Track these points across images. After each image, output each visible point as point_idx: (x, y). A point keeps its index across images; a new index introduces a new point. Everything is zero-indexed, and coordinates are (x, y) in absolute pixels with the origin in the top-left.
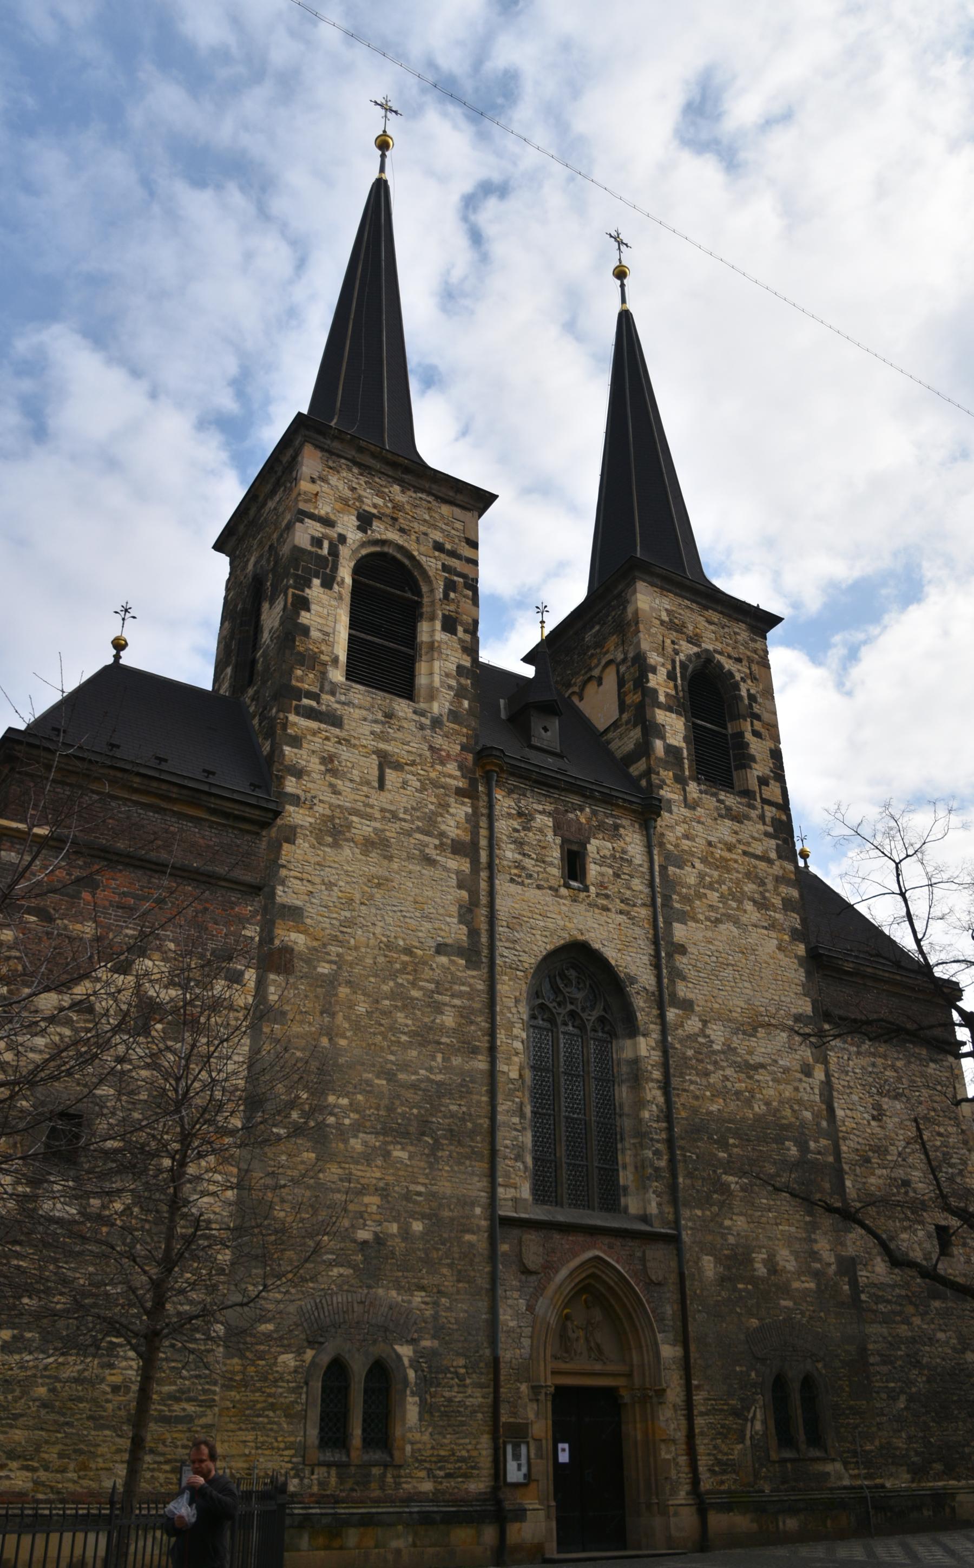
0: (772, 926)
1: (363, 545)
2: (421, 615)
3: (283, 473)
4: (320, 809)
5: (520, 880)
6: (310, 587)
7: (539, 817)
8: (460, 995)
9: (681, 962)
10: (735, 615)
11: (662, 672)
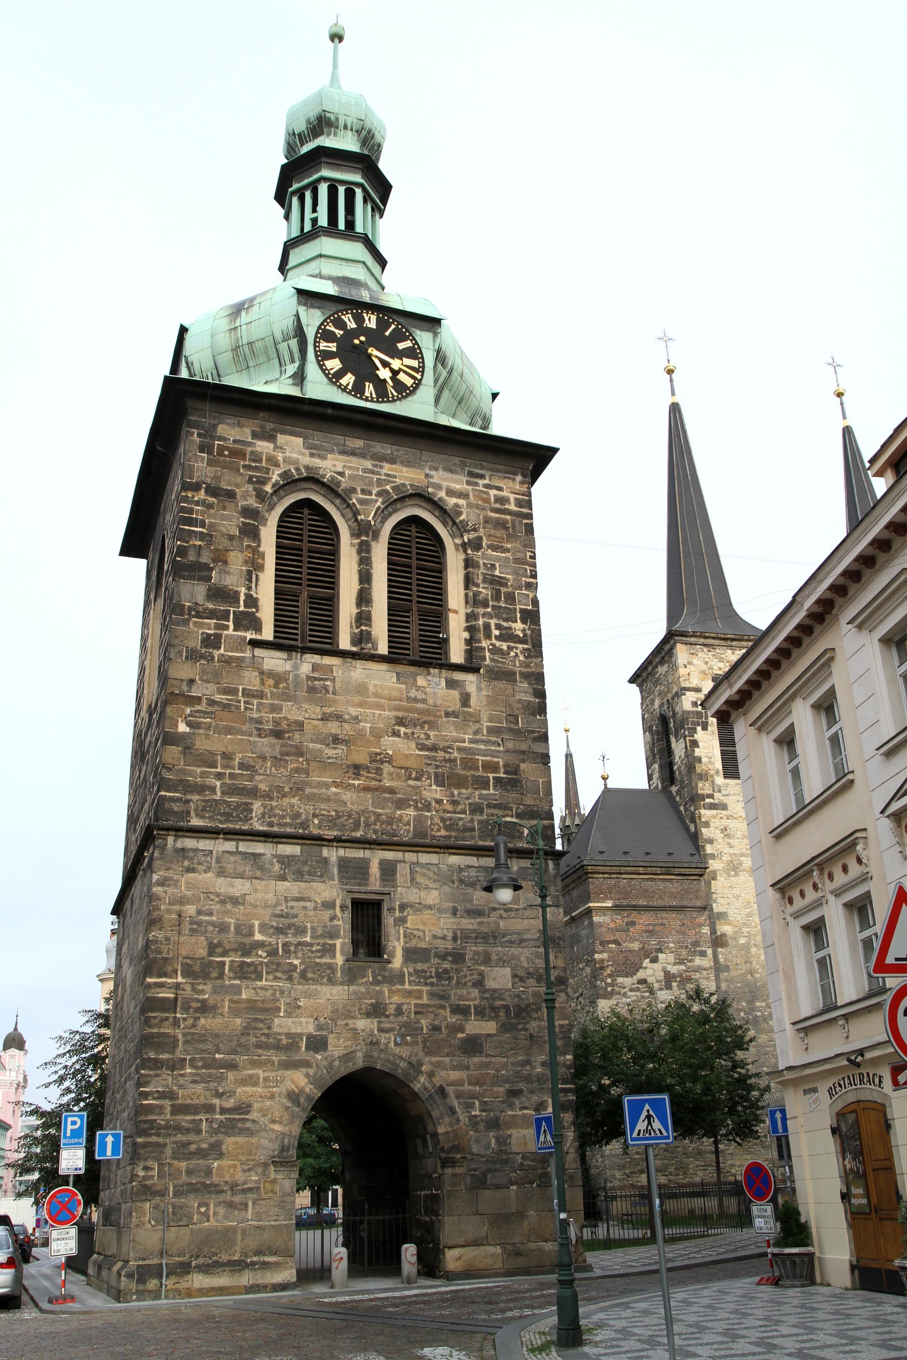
4: (725, 858)
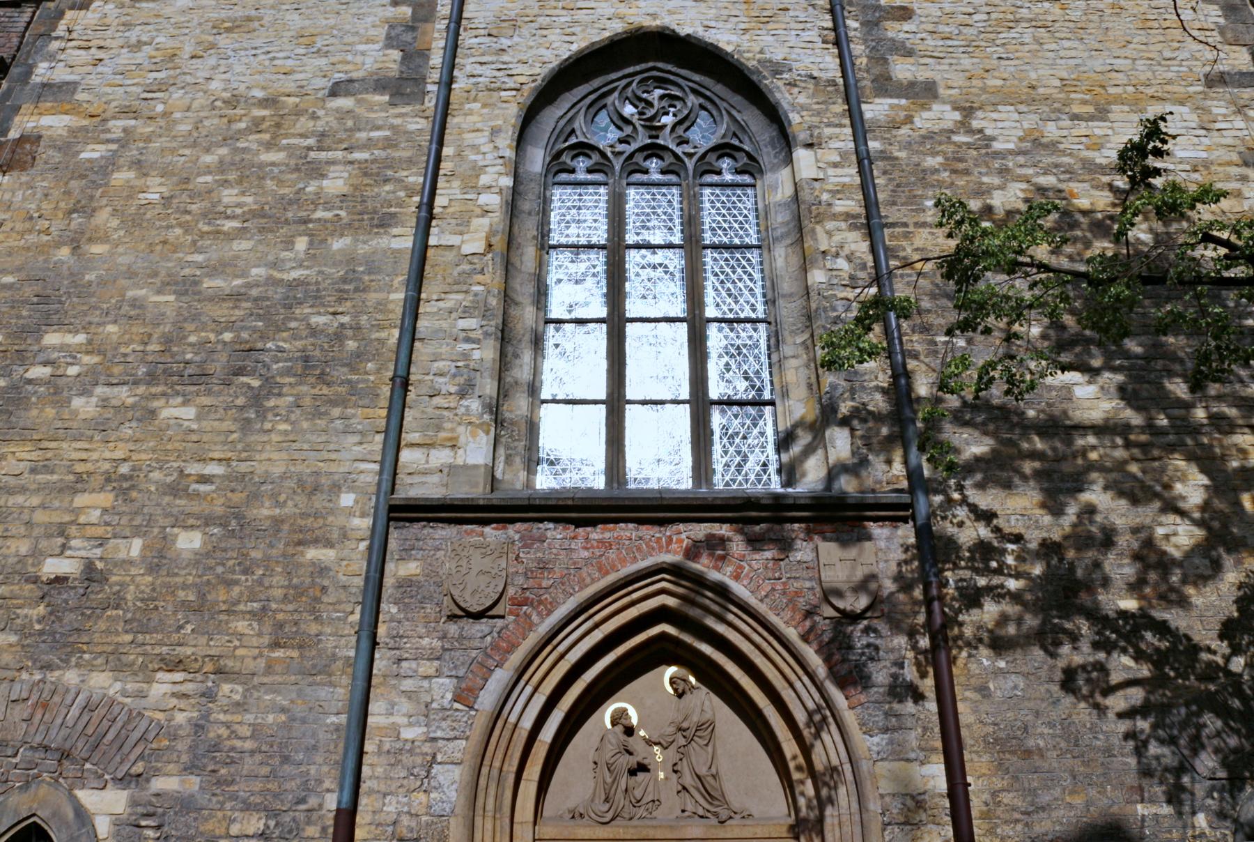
8: (369, 144)
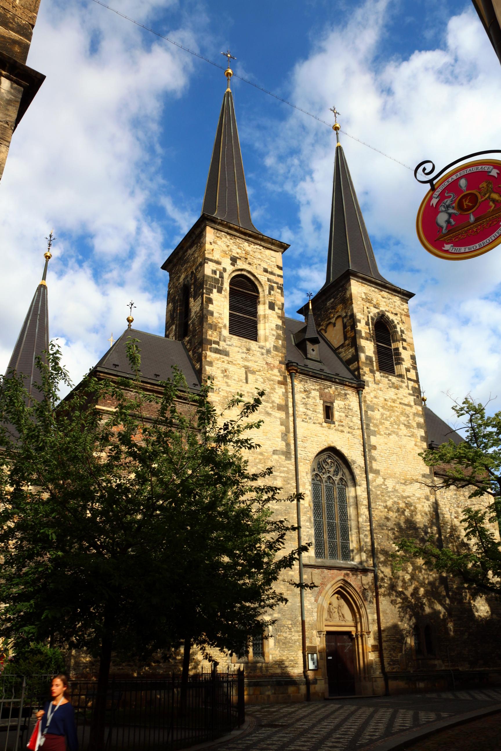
0: (413, 435)
1: (234, 271)
2: (259, 302)
3: (196, 238)
4: (222, 393)
5: (306, 420)
6: (212, 293)
7: (313, 392)
9: (374, 453)
10: (394, 293)
11: (363, 322)
